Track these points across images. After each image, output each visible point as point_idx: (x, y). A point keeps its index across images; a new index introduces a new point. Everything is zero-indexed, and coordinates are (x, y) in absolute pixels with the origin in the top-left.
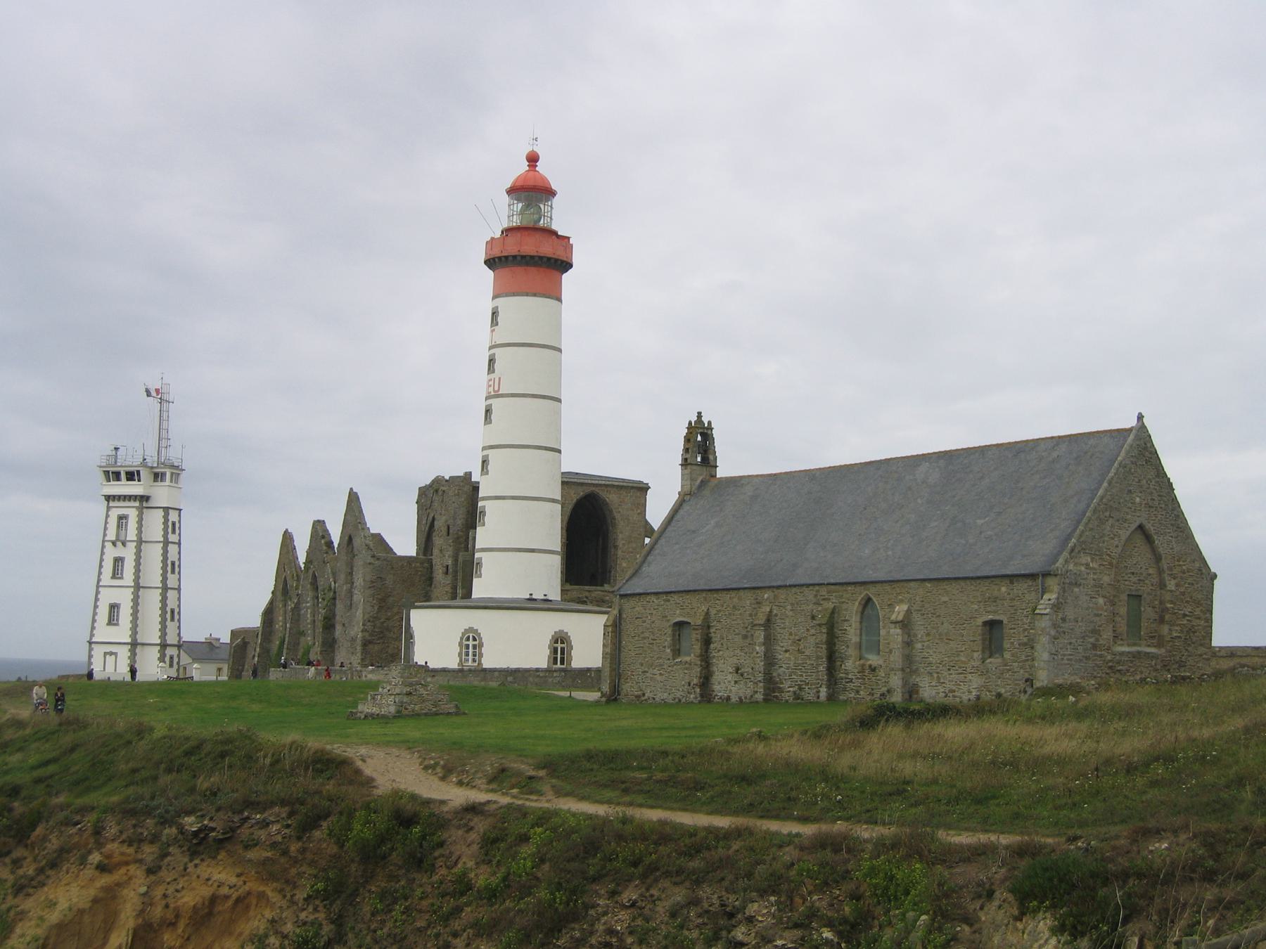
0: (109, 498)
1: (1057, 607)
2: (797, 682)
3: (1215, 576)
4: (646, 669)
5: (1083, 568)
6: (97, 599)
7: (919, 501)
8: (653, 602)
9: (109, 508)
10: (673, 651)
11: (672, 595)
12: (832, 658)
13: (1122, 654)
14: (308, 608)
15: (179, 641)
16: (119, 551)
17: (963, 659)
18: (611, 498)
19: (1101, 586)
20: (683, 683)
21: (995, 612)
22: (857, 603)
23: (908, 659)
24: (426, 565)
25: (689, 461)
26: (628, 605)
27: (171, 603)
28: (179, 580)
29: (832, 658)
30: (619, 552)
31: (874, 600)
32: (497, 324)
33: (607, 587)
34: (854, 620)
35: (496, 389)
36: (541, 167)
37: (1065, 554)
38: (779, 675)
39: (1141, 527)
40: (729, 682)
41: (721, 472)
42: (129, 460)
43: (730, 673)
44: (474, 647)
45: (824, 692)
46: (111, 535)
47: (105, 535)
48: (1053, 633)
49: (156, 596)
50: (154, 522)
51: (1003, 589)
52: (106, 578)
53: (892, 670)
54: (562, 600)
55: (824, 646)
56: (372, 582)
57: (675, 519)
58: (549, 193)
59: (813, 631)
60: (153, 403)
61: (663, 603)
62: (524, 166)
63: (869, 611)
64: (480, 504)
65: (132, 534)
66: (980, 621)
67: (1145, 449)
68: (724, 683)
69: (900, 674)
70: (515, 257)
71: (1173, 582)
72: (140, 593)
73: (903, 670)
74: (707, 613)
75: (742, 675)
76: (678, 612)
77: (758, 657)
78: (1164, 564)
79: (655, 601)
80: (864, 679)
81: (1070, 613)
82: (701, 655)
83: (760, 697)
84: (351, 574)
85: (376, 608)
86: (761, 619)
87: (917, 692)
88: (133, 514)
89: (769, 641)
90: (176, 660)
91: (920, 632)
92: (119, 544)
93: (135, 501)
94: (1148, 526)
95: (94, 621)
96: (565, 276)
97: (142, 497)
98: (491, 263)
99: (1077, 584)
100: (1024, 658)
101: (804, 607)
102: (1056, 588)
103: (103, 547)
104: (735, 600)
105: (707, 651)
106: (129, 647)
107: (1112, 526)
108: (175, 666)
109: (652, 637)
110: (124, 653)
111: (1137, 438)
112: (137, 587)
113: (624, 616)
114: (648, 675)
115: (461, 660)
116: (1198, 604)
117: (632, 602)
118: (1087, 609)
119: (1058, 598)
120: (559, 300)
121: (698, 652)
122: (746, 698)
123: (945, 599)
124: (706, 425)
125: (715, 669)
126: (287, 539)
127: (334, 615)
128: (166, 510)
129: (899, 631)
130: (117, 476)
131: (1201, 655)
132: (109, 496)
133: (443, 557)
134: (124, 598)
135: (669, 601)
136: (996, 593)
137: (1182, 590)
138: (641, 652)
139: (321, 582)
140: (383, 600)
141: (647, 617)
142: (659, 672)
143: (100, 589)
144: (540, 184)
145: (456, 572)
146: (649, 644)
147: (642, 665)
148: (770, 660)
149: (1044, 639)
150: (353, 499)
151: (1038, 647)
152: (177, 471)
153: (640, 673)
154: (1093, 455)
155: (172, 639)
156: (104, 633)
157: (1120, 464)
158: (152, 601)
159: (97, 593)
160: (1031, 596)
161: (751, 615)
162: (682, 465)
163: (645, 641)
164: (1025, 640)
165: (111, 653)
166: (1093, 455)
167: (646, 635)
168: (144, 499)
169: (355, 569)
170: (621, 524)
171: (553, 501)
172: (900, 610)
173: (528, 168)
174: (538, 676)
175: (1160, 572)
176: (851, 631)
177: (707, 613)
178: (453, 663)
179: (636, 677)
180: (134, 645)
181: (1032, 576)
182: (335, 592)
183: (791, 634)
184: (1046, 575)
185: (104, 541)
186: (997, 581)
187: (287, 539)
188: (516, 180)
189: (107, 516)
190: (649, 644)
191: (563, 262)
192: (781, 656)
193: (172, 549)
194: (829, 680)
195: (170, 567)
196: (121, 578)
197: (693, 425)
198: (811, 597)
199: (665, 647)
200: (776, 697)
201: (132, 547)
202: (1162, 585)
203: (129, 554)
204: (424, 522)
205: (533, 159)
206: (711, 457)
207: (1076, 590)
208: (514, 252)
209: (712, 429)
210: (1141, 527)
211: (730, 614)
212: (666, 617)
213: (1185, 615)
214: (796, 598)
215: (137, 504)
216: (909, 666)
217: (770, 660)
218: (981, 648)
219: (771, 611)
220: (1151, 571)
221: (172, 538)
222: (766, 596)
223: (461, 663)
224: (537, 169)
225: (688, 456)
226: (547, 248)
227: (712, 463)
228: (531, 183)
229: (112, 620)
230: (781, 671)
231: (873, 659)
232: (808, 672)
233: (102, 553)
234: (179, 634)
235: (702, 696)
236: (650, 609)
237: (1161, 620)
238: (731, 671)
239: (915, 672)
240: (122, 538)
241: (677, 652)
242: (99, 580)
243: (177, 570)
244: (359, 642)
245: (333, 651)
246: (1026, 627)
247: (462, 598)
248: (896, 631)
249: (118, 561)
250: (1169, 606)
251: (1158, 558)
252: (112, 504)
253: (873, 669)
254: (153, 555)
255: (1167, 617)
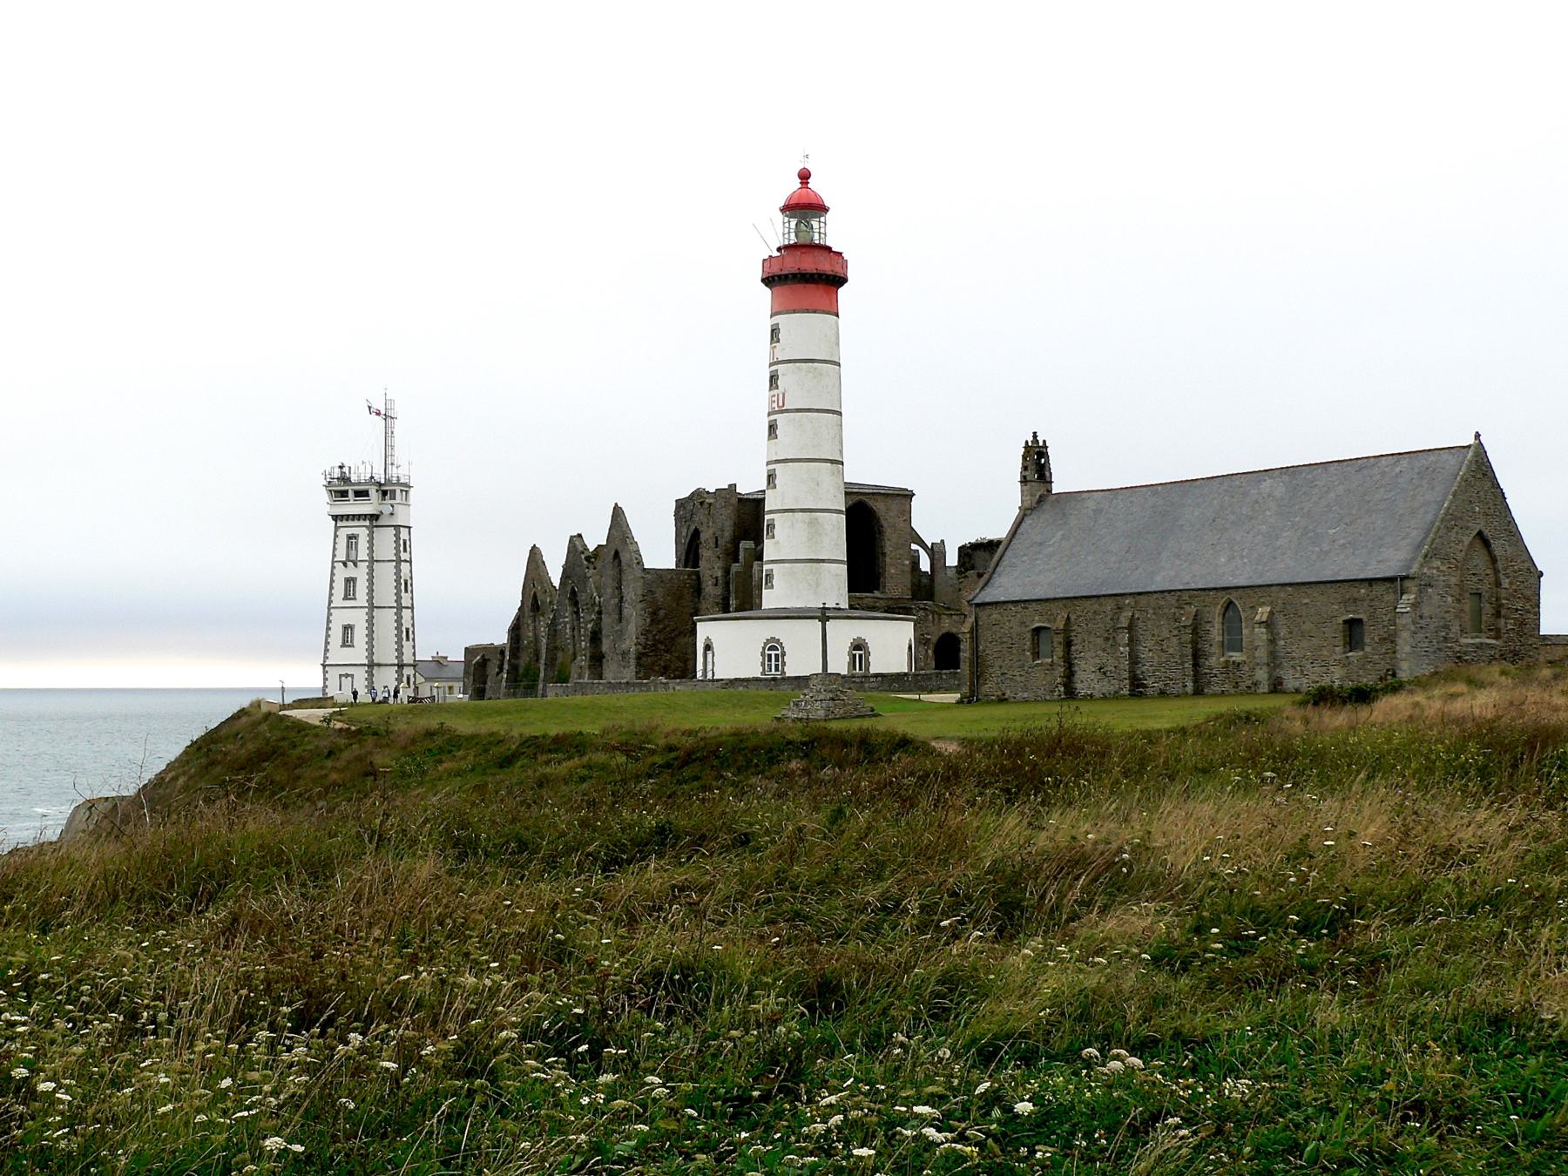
0: (336, 518)
1: (1415, 605)
3: (1541, 574)
5: (1435, 571)
6: (329, 621)
7: (1268, 513)
9: (337, 528)
10: (1033, 654)
12: (1197, 656)
13: (1468, 645)
14: (566, 623)
15: (415, 661)
16: (351, 572)
17: (1325, 653)
18: (879, 506)
19: (1449, 586)
21: (1354, 612)
22: (1219, 607)
23: (1273, 655)
24: (694, 577)
25: (1028, 478)
26: (983, 614)
27: (406, 623)
28: (412, 599)
29: (1197, 656)
30: (887, 559)
31: (1237, 603)
32: (778, 341)
33: (877, 594)
34: (1218, 620)
35: (781, 404)
36: (812, 183)
37: (1420, 559)
38: (1143, 672)
39: (1480, 534)
41: (1056, 488)
42: (359, 474)
44: (777, 655)
45: (1190, 685)
46: (341, 556)
47: (334, 556)
48: (1413, 628)
49: (390, 615)
50: (385, 539)
51: (1363, 591)
52: (338, 599)
53: (1258, 664)
54: (851, 607)
55: (1189, 646)
56: (644, 596)
57: (1019, 532)
58: (819, 209)
59: (1176, 632)
60: (380, 421)
62: (797, 183)
63: (1230, 613)
64: (767, 517)
65: (363, 554)
66: (1340, 620)
67: (1483, 463)
68: (1086, 680)
69: (1265, 669)
70: (794, 275)
71: (1507, 581)
72: (374, 614)
73: (1268, 665)
74: (1068, 618)
75: (1105, 673)
76: (1037, 618)
78: (1500, 565)
81: (1426, 611)
82: (1063, 657)
83: (1126, 692)
84: (619, 588)
85: (648, 620)
86: (1124, 622)
87: (1281, 684)
88: (363, 534)
89: (1132, 642)
90: (412, 680)
91: (1283, 632)
92: (350, 564)
93: (365, 520)
94: (1486, 532)
95: (327, 643)
96: (841, 290)
97: (372, 515)
98: (768, 281)
99: (1430, 585)
100: (1384, 651)
101: (1166, 611)
102: (1415, 589)
103: (333, 567)
104: (1096, 606)
105: (1068, 654)
106: (396, 668)
107: (1457, 533)
108: (412, 686)
110: (361, 675)
111: (1477, 454)
112: (372, 607)
113: (980, 623)
115: (764, 669)
116: (1528, 599)
117: (988, 611)
118: (1439, 607)
119: (1415, 598)
120: (838, 316)
121: (1061, 654)
123: (1306, 601)
124: (1041, 444)
125: (1076, 668)
126: (535, 557)
127: (600, 630)
128: (397, 527)
129: (1264, 630)
130: (344, 494)
131: (1531, 645)
132: (337, 516)
133: (710, 566)
134: (359, 619)
136: (1356, 595)
137: (1514, 587)
139: (582, 597)
140: (654, 613)
143: (332, 611)
144: (814, 201)
145: (727, 584)
147: (1001, 667)
148: (1134, 660)
149: (1405, 635)
150: (618, 513)
151: (1399, 641)
152: (406, 488)
154: (1435, 470)
155: (407, 659)
156: (339, 655)
157: (1462, 479)
158: (386, 620)
159: (329, 614)
160: (1390, 597)
161: (1112, 619)
162: (1021, 482)
164: (1385, 635)
165: (347, 676)
166: (1435, 470)
167: (1005, 640)
168: (374, 517)
169: (624, 583)
170: (888, 532)
171: (839, 512)
172: (1263, 612)
173: (800, 186)
174: (854, 682)
175: (1496, 571)
176: (1215, 633)
177: (1068, 618)
178: (756, 672)
180: (371, 665)
181: (1391, 580)
182: (600, 607)
183: (1153, 635)
184: (1403, 578)
185: (333, 562)
186: (1356, 584)
187: (535, 557)
188: (790, 198)
189: (336, 536)
191: (840, 277)
192: (1144, 655)
193: (404, 567)
194: (1194, 676)
195: (404, 585)
196: (355, 599)
197: (1030, 444)
198: (1174, 602)
200: (1141, 692)
201: (363, 567)
202: (1498, 584)
203: (361, 574)
204: (684, 534)
205: (805, 176)
206: (1047, 474)
207: (1430, 590)
208: (794, 271)
209: (1047, 447)
210: (1480, 534)
211: (1091, 619)
213: (1517, 610)
215: (367, 523)
216: (1274, 661)
217: (1134, 660)
218: (1342, 643)
219: (1133, 616)
220: (1488, 572)
221: (404, 556)
222: (1127, 601)
223: (763, 673)
224: (809, 186)
225: (1026, 473)
226: (825, 266)
227: (1048, 480)
228: (805, 201)
229: (347, 642)
230: (1144, 669)
231: (1237, 657)
233: (333, 574)
234: (414, 654)
235: (1066, 693)
237: (1498, 615)
239: (1279, 666)
240: (353, 558)
241: (1036, 655)
242: (330, 602)
243: (409, 588)
244: (632, 655)
245: (601, 666)
246: (1385, 623)
247: (737, 610)
248: (1261, 632)
249: (350, 581)
250: (1504, 602)
251: (1494, 560)
252: (339, 524)
253: (1238, 665)
254: (385, 573)
255: (1503, 612)
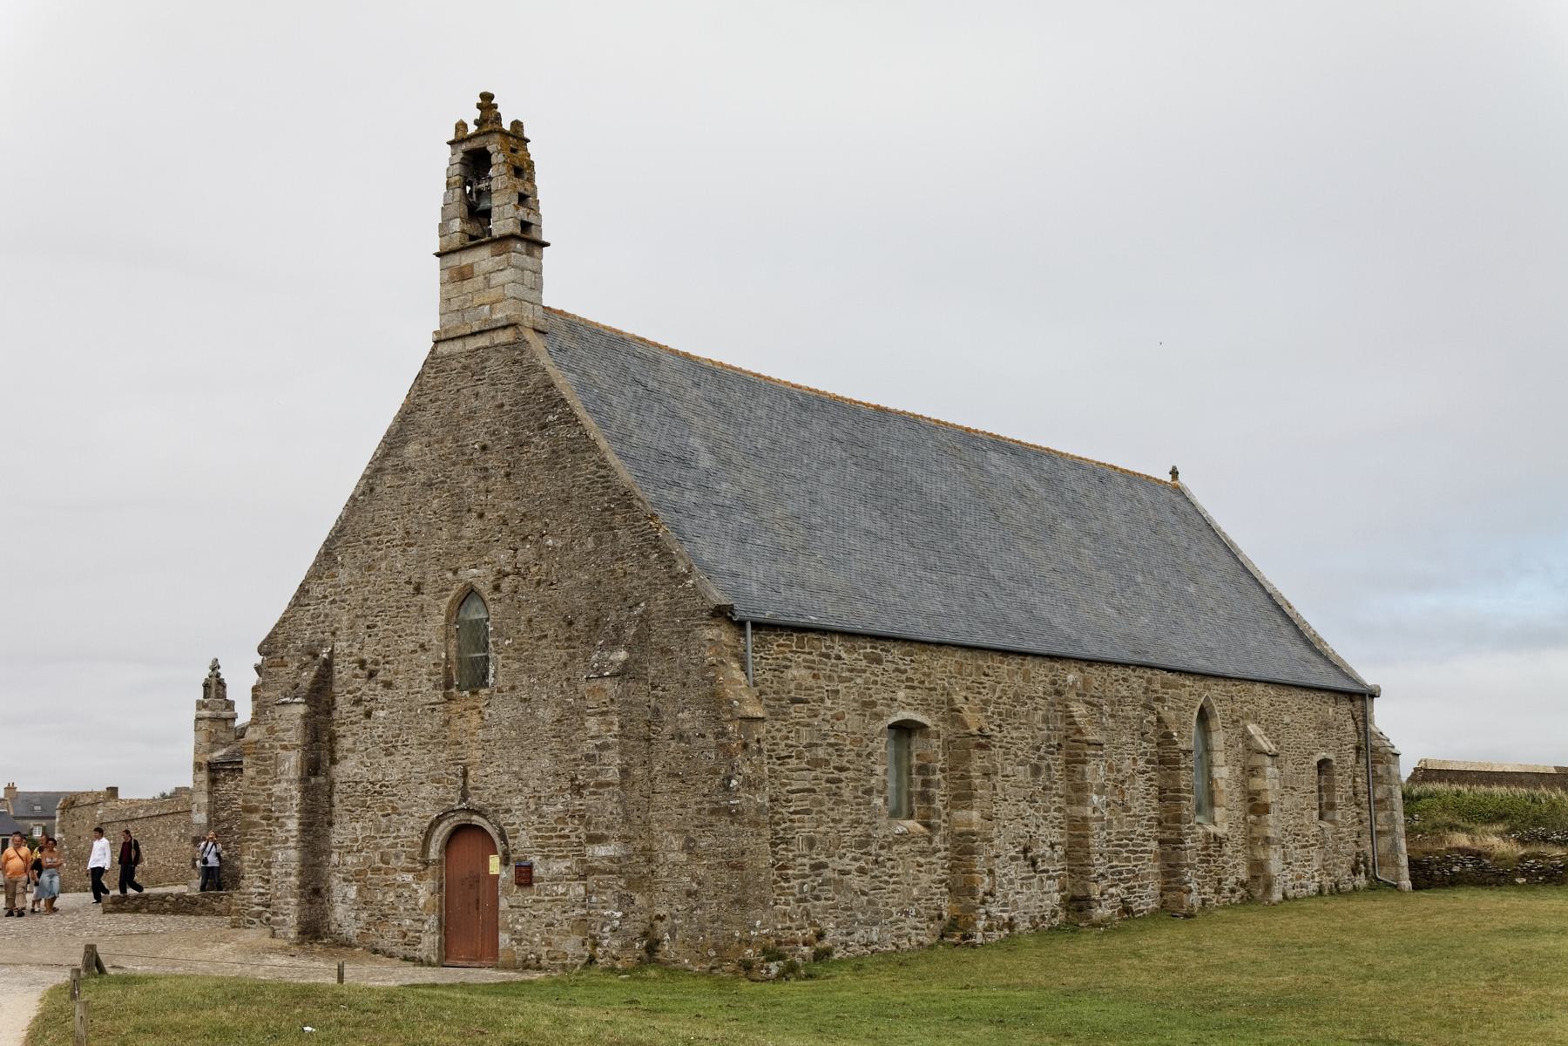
2: (1121, 873)
4: (823, 858)
8: (839, 658)
11: (888, 645)
20: (915, 892)
40: (1011, 882)
43: (1013, 859)
61: (864, 663)
77: (1097, 820)
79: (844, 655)
80: (1208, 862)
104: (1018, 679)
109: (835, 759)
114: (828, 873)
122: (1043, 917)
135: (879, 661)
138: (806, 804)
141: (822, 700)
142: (857, 865)
146: (828, 781)
148: (1078, 831)
153: (807, 870)
163: (818, 772)
179: (794, 883)
183: (1111, 768)
190: (828, 781)
199: (869, 792)
212: (874, 704)
214: (1117, 690)
217: (1078, 831)
222: (1070, 678)
232: (1137, 852)
236: (830, 678)
238: (1013, 854)
